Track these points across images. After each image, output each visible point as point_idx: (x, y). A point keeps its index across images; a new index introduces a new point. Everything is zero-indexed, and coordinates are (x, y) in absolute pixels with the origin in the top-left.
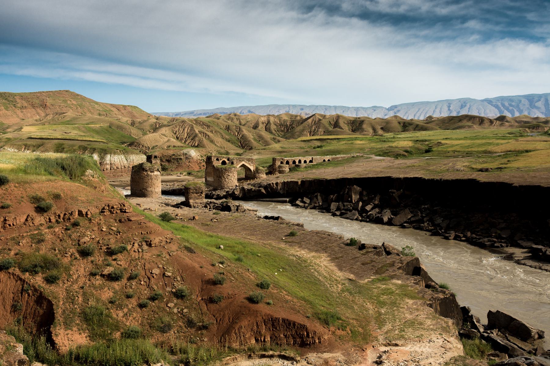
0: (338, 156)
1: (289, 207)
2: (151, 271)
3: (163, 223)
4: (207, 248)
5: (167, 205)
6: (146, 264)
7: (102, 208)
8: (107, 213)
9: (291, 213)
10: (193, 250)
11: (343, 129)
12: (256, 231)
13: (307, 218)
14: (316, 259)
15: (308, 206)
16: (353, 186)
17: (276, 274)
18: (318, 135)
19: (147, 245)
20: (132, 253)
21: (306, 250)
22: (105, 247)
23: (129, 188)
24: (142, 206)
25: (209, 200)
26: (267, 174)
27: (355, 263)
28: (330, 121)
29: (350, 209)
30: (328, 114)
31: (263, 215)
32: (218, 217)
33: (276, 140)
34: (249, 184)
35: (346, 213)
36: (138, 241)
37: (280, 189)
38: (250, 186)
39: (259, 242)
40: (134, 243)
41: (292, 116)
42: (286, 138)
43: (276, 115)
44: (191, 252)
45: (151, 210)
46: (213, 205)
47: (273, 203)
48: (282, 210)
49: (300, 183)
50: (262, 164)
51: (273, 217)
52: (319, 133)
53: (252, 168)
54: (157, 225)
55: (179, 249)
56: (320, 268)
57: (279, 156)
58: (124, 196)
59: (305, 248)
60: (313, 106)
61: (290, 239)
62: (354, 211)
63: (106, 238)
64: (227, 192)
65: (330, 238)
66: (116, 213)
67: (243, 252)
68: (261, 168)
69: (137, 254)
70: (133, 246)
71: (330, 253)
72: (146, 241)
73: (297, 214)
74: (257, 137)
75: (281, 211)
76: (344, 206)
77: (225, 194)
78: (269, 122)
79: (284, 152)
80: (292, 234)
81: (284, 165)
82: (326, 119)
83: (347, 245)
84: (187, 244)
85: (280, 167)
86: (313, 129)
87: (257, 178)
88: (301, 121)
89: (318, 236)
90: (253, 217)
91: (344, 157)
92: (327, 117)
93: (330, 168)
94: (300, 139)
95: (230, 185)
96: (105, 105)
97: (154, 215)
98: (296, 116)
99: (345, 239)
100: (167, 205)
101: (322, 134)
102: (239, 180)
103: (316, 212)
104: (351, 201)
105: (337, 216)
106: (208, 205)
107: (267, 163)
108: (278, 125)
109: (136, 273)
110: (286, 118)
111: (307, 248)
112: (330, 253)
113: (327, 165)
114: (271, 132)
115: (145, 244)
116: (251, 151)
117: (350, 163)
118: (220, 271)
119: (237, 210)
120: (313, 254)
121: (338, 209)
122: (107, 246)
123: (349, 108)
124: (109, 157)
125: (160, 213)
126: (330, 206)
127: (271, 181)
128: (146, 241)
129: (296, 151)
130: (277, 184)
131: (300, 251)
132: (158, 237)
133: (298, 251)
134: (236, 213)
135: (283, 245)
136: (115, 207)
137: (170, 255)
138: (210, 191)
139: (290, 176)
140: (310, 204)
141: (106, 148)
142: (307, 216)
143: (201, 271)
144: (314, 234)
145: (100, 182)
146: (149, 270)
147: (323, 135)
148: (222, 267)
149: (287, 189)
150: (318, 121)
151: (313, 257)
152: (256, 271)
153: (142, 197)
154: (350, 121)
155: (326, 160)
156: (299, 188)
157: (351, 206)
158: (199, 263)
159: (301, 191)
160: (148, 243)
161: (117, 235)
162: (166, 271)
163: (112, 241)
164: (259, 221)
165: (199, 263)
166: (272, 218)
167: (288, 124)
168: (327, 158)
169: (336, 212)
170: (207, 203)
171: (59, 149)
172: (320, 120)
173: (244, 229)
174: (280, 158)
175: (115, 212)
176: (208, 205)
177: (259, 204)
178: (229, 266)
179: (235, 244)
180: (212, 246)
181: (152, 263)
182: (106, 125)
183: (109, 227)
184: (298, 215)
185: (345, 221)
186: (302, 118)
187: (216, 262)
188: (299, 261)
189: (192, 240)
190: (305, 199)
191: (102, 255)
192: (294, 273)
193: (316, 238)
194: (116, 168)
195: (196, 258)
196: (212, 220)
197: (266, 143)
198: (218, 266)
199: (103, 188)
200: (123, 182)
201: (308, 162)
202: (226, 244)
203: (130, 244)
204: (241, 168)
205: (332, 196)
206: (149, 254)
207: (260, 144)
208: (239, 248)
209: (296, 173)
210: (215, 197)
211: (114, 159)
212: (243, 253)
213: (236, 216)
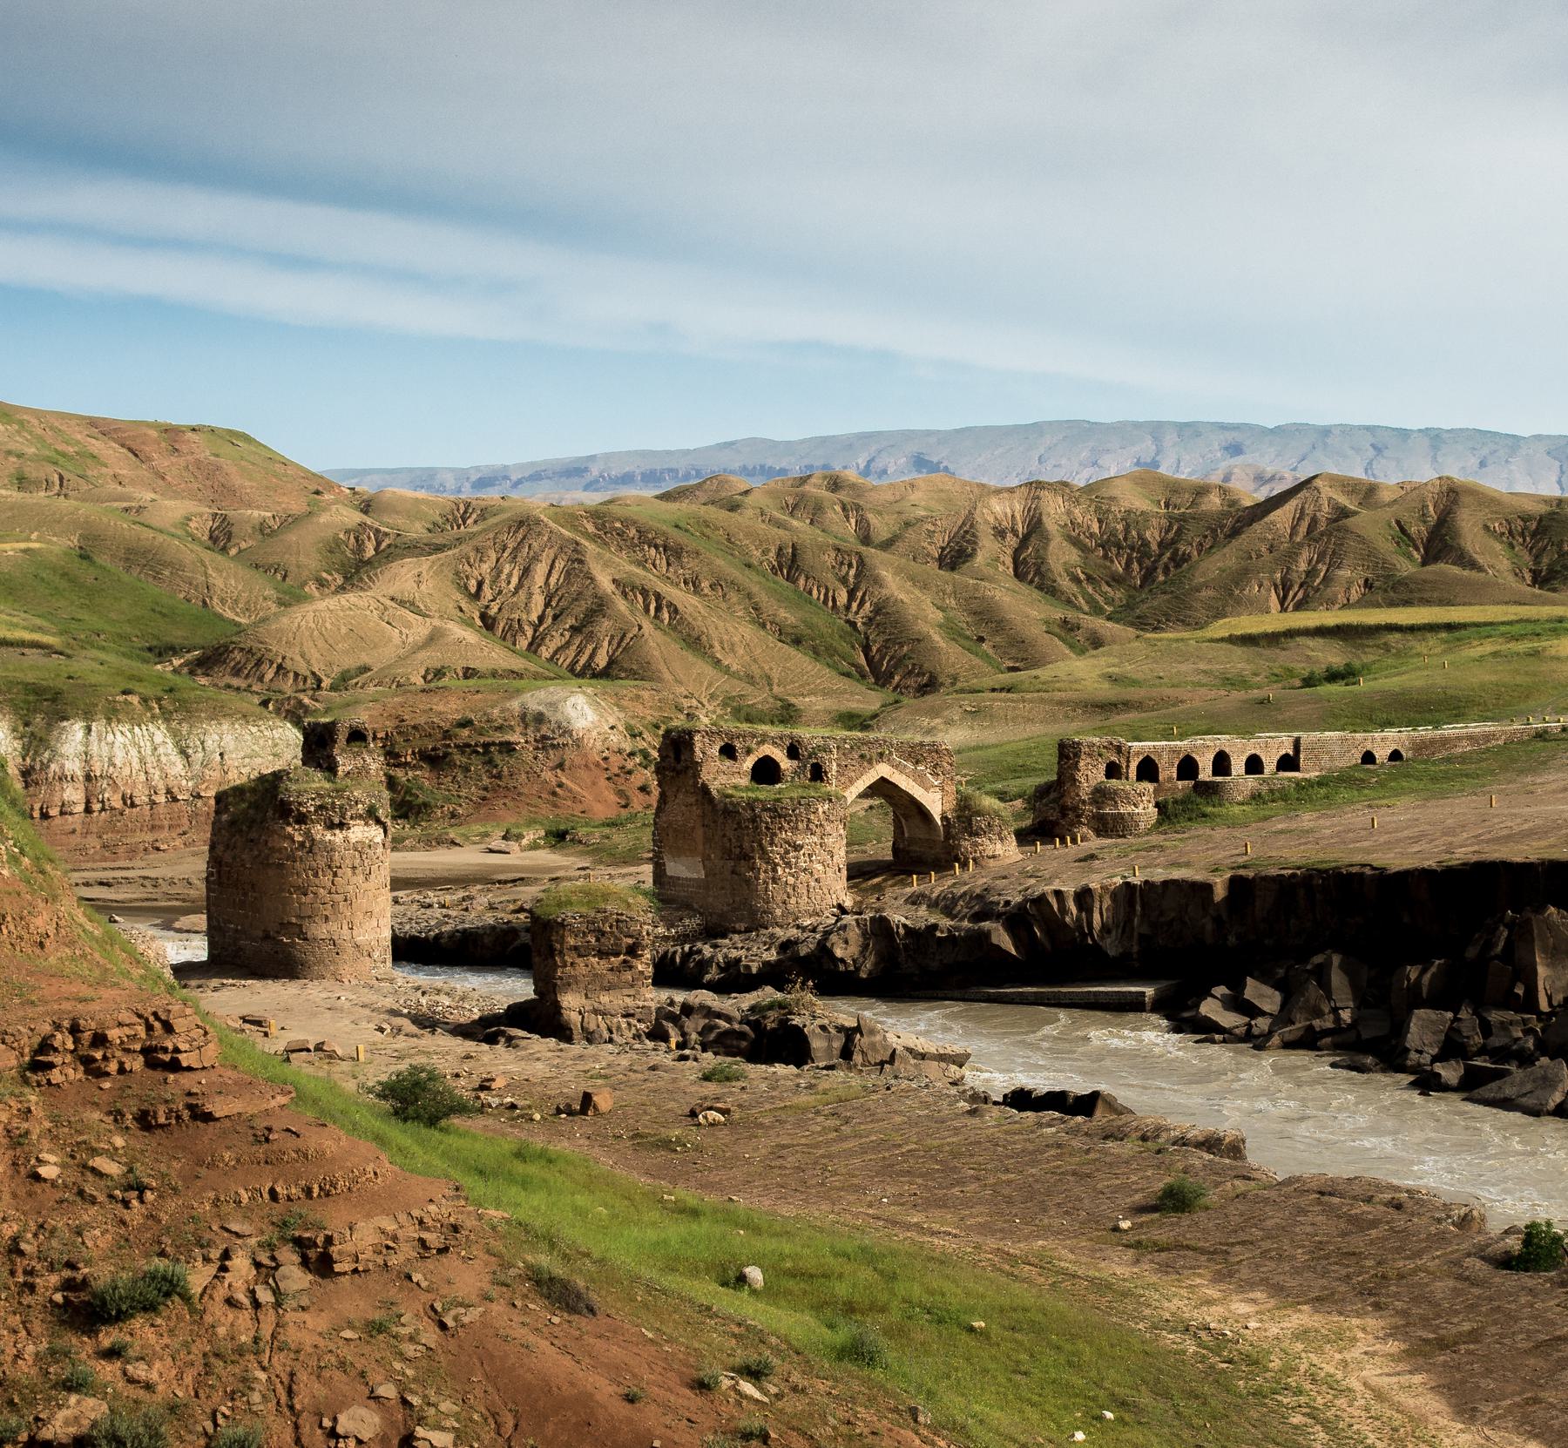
0: (1449, 730)
1: (1154, 1036)
2: (327, 1423)
3: (399, 1134)
4: (670, 1281)
5: (427, 1022)
6: (303, 1376)
7: (37, 1040)
8: (66, 1073)
9: (1171, 1070)
10: (579, 1296)
11: (1480, 569)
12: (959, 1182)
13: (1263, 1104)
14: (1319, 1351)
15: (1270, 1033)
16: (1541, 909)
17: (1080, 1436)
18: (1330, 603)
19: (305, 1263)
20: (216, 1310)
21: (1258, 1295)
22: (54, 1279)
23: (200, 921)
24: (274, 1031)
25: (680, 997)
26: (1024, 837)
27: (1552, 1373)
28: (1405, 518)
29: (1522, 1050)
30: (1390, 476)
31: (999, 1082)
32: (731, 1095)
33: (1080, 636)
34: (914, 900)
35: (1500, 1075)
36: (253, 1241)
37: (1105, 929)
38: (923, 911)
39: (978, 1247)
40: (226, 1255)
41: (1174, 488)
42: (1141, 623)
43: (1080, 481)
44: (572, 1310)
45: (332, 1056)
46: (702, 1022)
47: (1063, 1015)
48: (1116, 1052)
49: (1220, 893)
50: (997, 776)
51: (1063, 1094)
52: (1338, 590)
53: (936, 803)
54: (366, 1147)
55: (494, 1292)
56: (1342, 1402)
57: (1096, 731)
58: (168, 974)
59: (1251, 1285)
60: (1298, 430)
61: (1164, 1229)
62: (1544, 1060)
63: (58, 1222)
64: (786, 946)
65: (1400, 1220)
66: (122, 1070)
67: (883, 1310)
68: (989, 802)
69: (244, 1318)
70: (224, 1269)
71: (1404, 1313)
72: (299, 1243)
73: (1204, 1077)
74: (962, 619)
75: (1108, 1063)
76: (1486, 1029)
77: (772, 956)
78: (1035, 526)
79: (1127, 705)
80: (1175, 1201)
81: (1129, 784)
82: (1377, 506)
83: (1506, 1262)
84: (544, 1260)
85: (1101, 795)
86: (1303, 566)
87: (964, 865)
88: (1229, 522)
89: (1329, 1211)
90: (940, 1096)
91: (1488, 737)
92: (1386, 496)
93: (1402, 802)
94: (1221, 628)
95: (799, 903)
96: (54, 422)
97: (350, 1086)
98: (1201, 491)
99: (1495, 1227)
100: (427, 1022)
101: (1354, 596)
102: (858, 873)
103: (1318, 1066)
104: (1530, 1003)
105: (1445, 1088)
106: (669, 1026)
107: (1024, 770)
108: (1092, 544)
109: (240, 1431)
110: (1138, 502)
111: (1264, 1282)
112: (1404, 1313)
113: (1381, 784)
114: (1048, 589)
115: (296, 1258)
116: (929, 699)
117: (1521, 772)
118: (743, 1423)
119: (846, 1053)
120: (1303, 1318)
121: (1451, 1048)
122: (67, 1273)
123: (1514, 442)
124: (80, 735)
125: (381, 1072)
126: (1400, 1028)
127: (1049, 881)
128: (299, 1243)
129: (1199, 699)
130: (1084, 897)
131: (1223, 1301)
132: (369, 1216)
133: (1209, 1302)
134: (839, 1074)
135: (1118, 1267)
136: (114, 1034)
137: (443, 1326)
138: (682, 938)
139: (1161, 848)
140: (1283, 1017)
141: (60, 683)
142: (1265, 1092)
143: (630, 1421)
144: (1303, 1201)
145: (23, 888)
146: (320, 1415)
147: (1362, 603)
148: (757, 1395)
149: (1145, 930)
150: (1331, 521)
151: (1302, 1334)
152: (960, 1418)
153: (275, 977)
154: (1526, 518)
155: (1381, 754)
156: (1217, 920)
157: (1528, 1032)
158: (615, 1371)
159: (1232, 940)
160: (312, 1254)
161: (126, 1204)
162: (421, 1420)
163: (99, 1239)
164: (975, 1121)
165: (615, 1371)
166: (1056, 1101)
167: (1153, 535)
168: (1384, 741)
169: (1438, 1068)
170: (664, 1014)
171: (184, 900)
172: (1342, 513)
173: (887, 1171)
174: (1105, 740)
175: (113, 1067)
176: (669, 1026)
177: (979, 1020)
178: (795, 1389)
179: (831, 1260)
180: (694, 1272)
181: (338, 1375)
182: (59, 544)
183: (80, 1158)
184: (1214, 1086)
185: (1489, 1123)
186: (1233, 503)
187: (717, 1369)
188: (1214, 1359)
189: (573, 1233)
190: (1254, 990)
191: (37, 1327)
192: (1186, 1434)
193: (1318, 1224)
194: (118, 804)
195: (600, 1344)
196: (693, 1114)
197: (1022, 654)
198: (734, 1388)
199: (42, 922)
200: (165, 888)
201: (1270, 765)
202: (782, 1258)
203: (206, 1260)
204: (867, 803)
205: (1413, 972)
206: (317, 1322)
207: (985, 657)
208: (856, 1281)
209: (1200, 829)
210: (712, 974)
211: (105, 749)
212: (883, 1310)
213: (841, 1092)
